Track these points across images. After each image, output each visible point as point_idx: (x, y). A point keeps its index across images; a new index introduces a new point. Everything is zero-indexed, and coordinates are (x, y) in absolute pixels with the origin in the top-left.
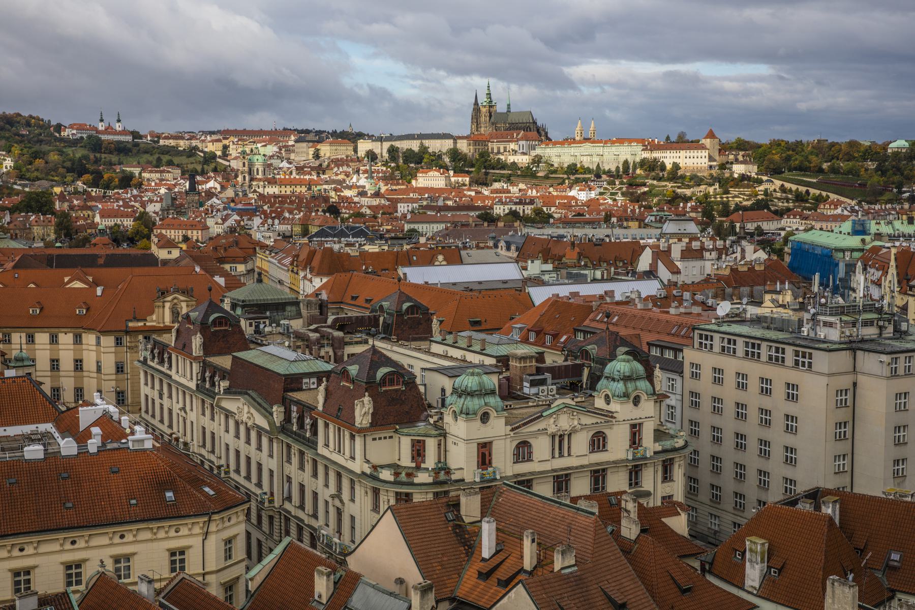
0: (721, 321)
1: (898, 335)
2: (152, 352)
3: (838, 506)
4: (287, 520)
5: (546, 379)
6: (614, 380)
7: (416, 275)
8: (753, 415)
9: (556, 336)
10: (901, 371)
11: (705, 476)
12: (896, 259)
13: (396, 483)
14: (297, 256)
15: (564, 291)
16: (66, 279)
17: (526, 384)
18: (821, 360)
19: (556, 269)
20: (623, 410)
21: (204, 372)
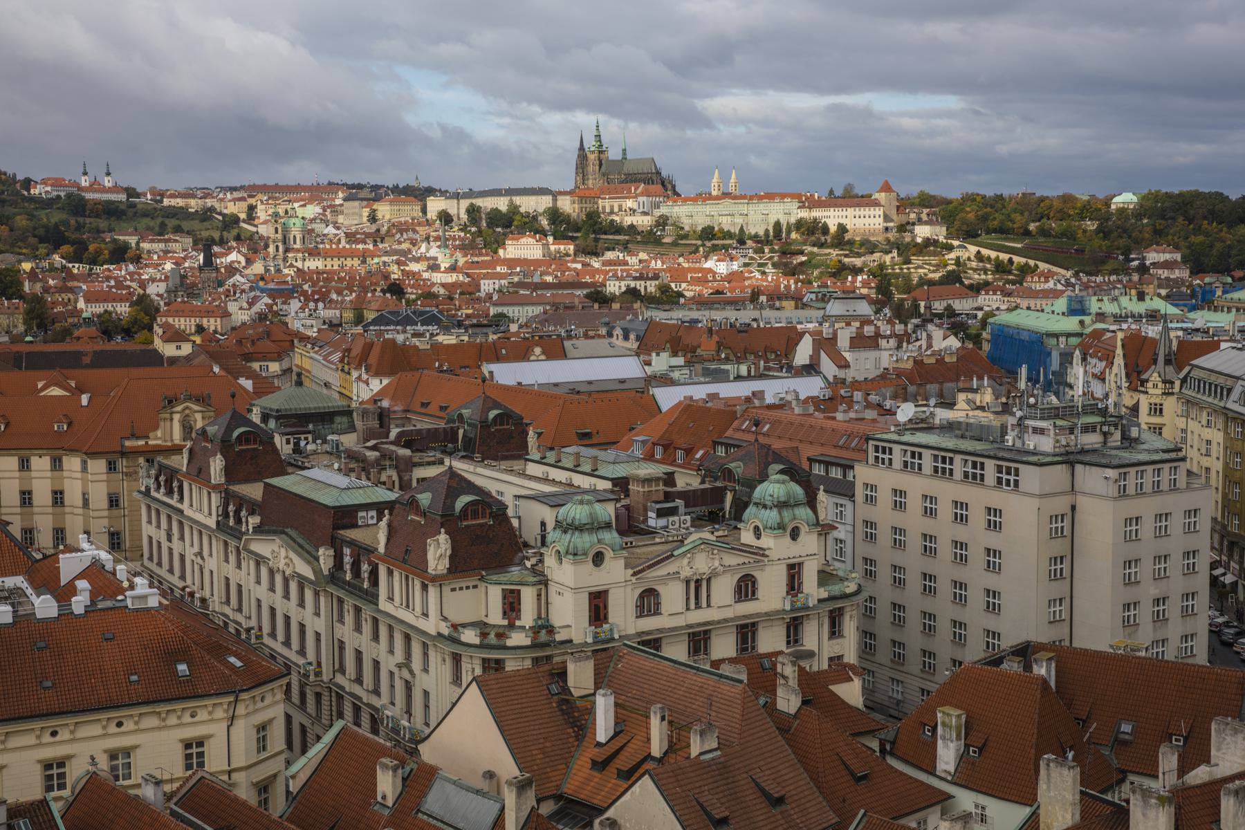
0: (903, 429)
2: (157, 479)
3: (1053, 665)
4: (340, 697)
5: (677, 507)
6: (765, 507)
7: (506, 374)
8: (945, 549)
9: (689, 451)
10: (1131, 490)
11: (884, 630)
12: (1123, 346)
13: (482, 646)
14: (349, 350)
15: (699, 392)
16: (40, 385)
17: (651, 514)
18: (1030, 477)
19: (689, 363)
20: (778, 547)
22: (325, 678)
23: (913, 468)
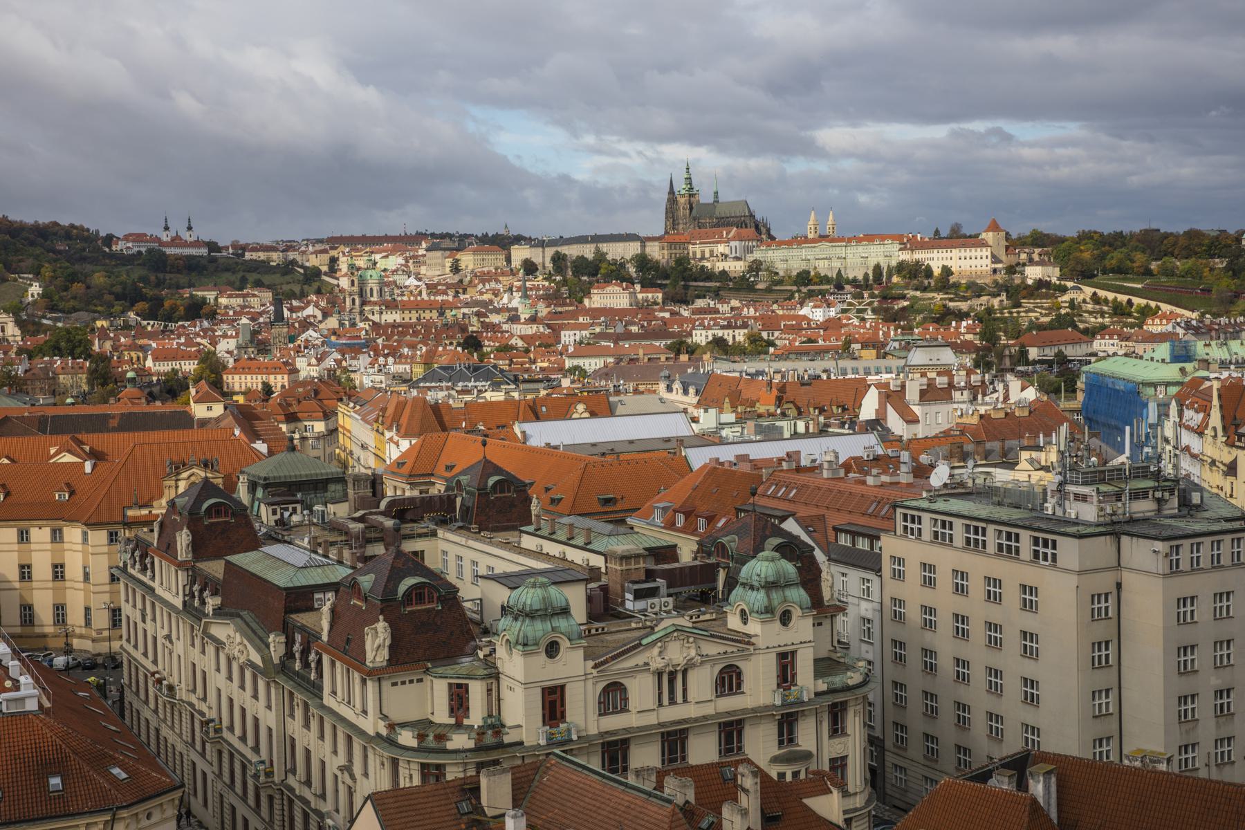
0: (936, 495)
1: (1185, 511)
2: (133, 554)
3: (1054, 779)
4: (291, 802)
6: (752, 588)
8: (977, 631)
10: (1185, 565)
12: (1220, 396)
13: (420, 750)
15: (726, 454)
16: (53, 451)
17: (629, 596)
18: (1069, 550)
19: (740, 421)
21: (193, 583)
22: (276, 779)
23: (944, 539)
